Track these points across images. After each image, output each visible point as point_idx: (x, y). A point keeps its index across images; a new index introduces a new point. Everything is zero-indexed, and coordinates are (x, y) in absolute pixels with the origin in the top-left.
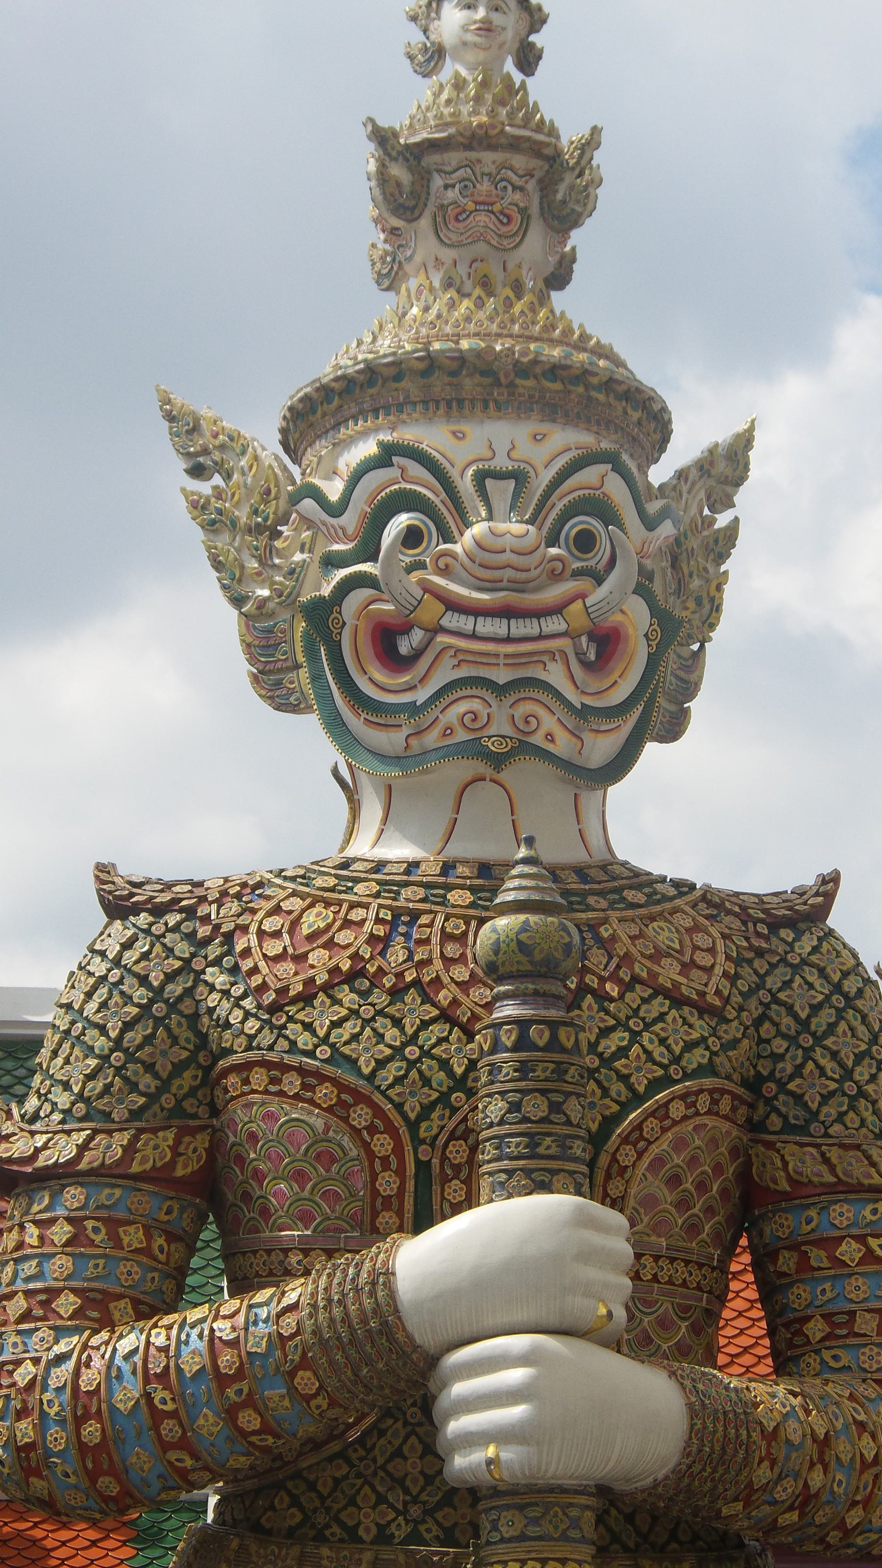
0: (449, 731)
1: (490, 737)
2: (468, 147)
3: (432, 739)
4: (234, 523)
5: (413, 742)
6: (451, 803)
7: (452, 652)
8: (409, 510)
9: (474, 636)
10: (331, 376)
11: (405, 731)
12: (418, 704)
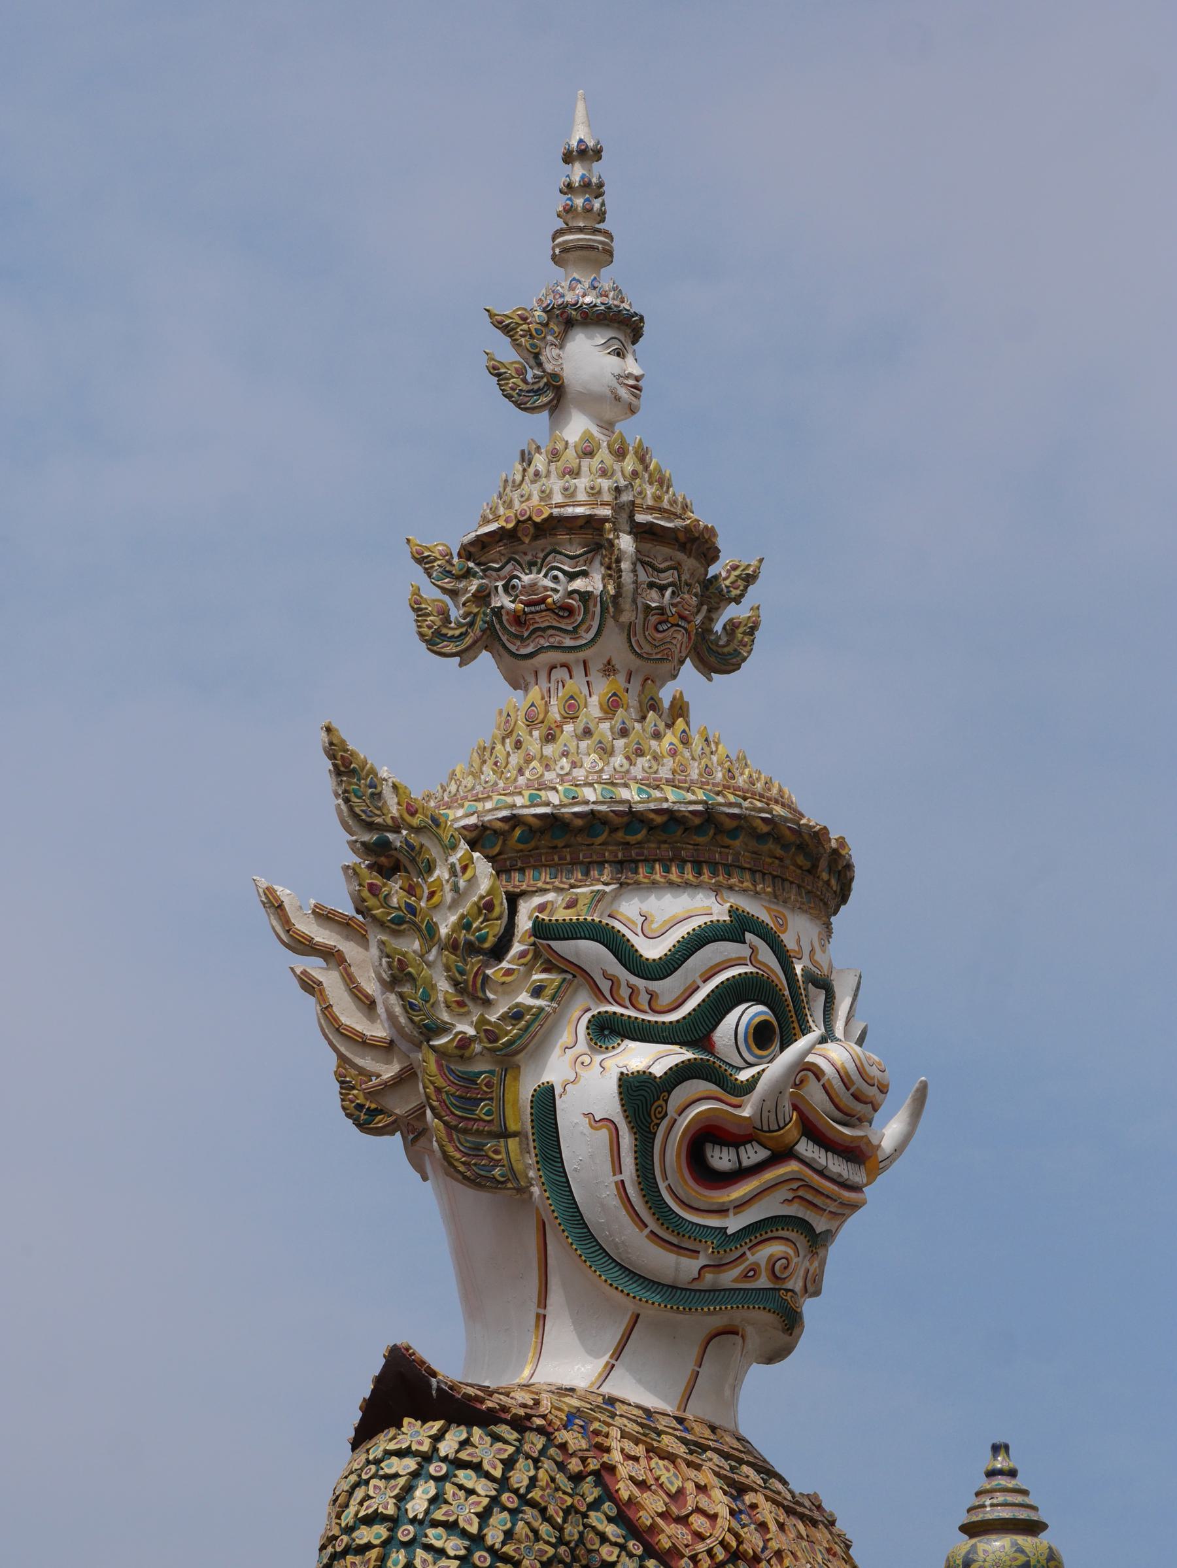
0: (751, 1273)
1: (787, 1290)
2: (683, 547)
3: (729, 1278)
4: (432, 929)
5: (709, 1277)
6: (695, 1352)
7: (795, 1185)
8: (759, 1002)
9: (821, 1173)
10: (652, 806)
11: (702, 1260)
12: (729, 1232)
